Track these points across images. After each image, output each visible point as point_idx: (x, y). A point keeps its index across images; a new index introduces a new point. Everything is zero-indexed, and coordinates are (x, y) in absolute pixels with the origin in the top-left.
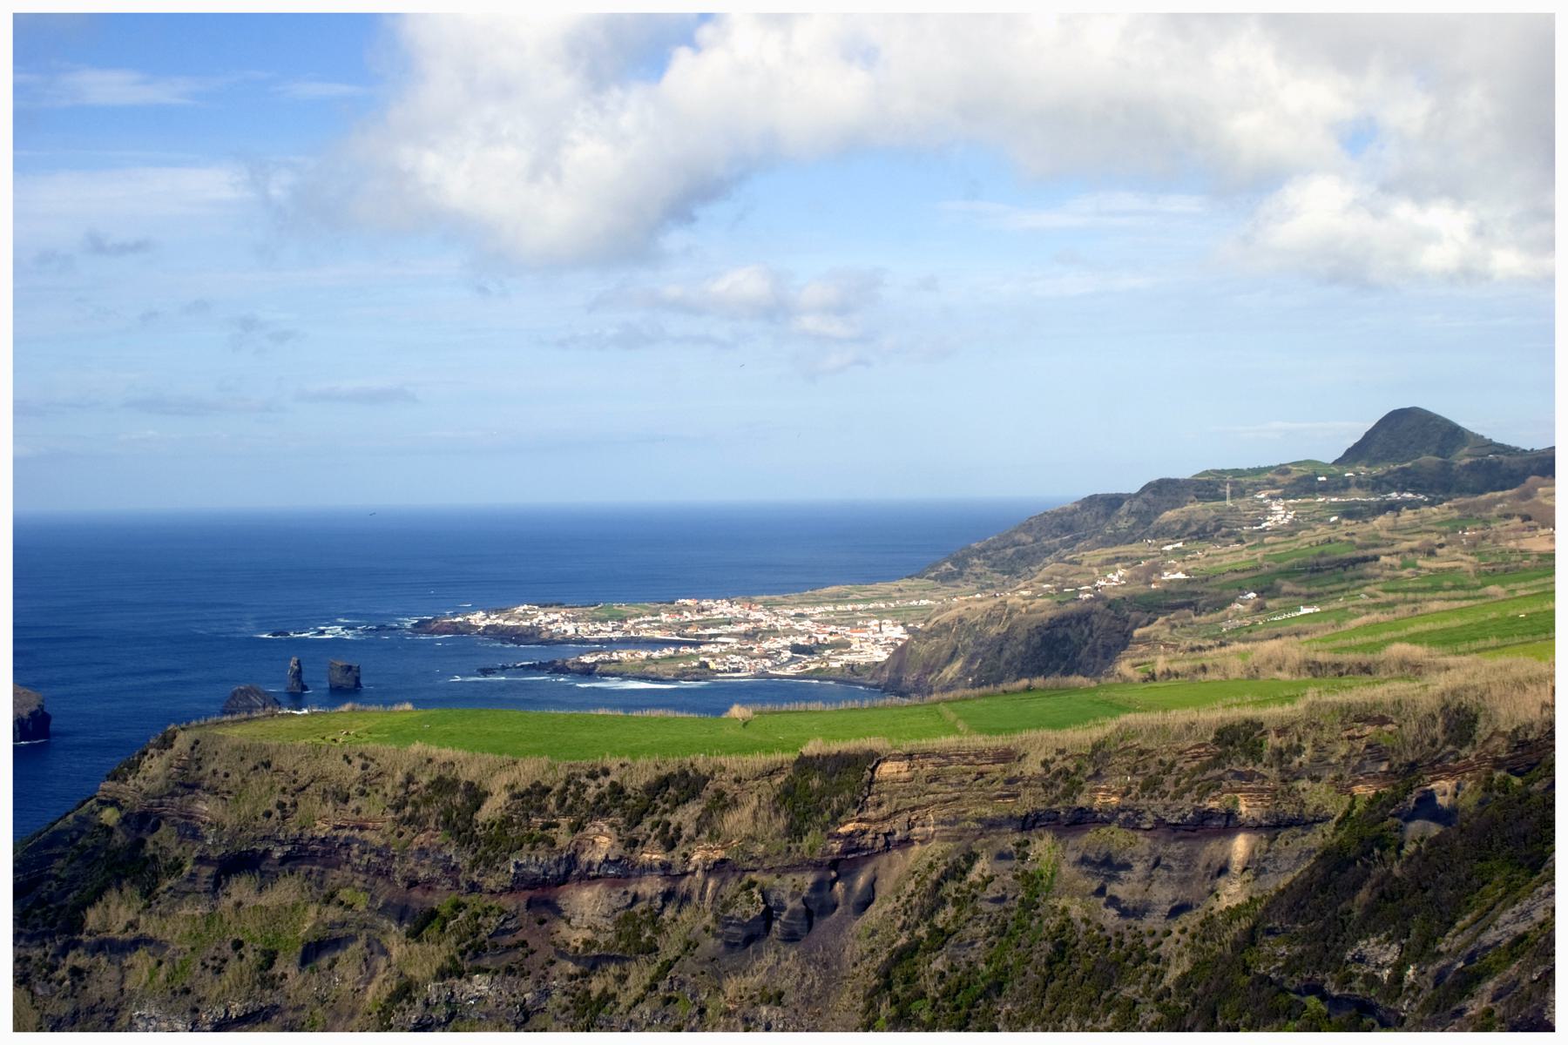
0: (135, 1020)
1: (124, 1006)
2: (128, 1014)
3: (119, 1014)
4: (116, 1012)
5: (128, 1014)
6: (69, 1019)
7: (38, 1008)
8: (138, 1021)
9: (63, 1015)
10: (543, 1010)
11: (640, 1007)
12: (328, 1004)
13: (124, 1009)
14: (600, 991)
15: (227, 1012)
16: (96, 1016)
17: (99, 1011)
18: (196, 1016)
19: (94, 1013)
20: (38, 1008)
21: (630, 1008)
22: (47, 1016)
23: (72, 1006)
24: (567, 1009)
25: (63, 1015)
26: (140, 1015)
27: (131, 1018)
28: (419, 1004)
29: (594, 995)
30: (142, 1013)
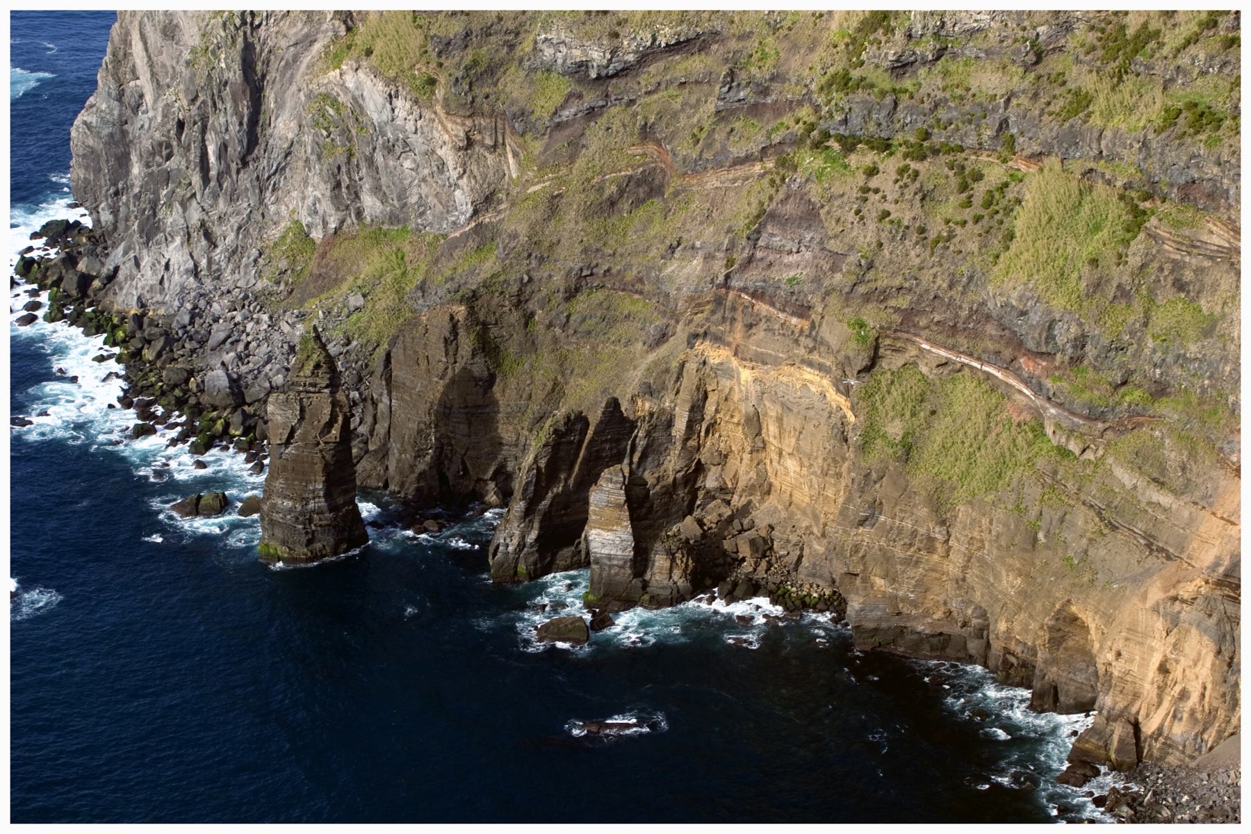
0: (540, 46)
1: (527, 27)
2: (531, 37)
3: (520, 38)
4: (517, 34)
5: (531, 37)
6: (460, 42)
7: (421, 27)
8: (544, 47)
9: (452, 36)
10: (1061, 49)
11: (1192, 50)
12: (782, 32)
13: (526, 31)
14: (1139, 27)
15: (654, 39)
16: (493, 39)
17: (496, 33)
18: (616, 42)
19: (490, 35)
20: (421, 27)
21: (1178, 51)
22: (432, 38)
23: (463, 25)
24: (1094, 48)
25: (452, 36)
26: (546, 39)
27: (536, 43)
28: (899, 36)
29: (1130, 32)
30: (549, 36)
